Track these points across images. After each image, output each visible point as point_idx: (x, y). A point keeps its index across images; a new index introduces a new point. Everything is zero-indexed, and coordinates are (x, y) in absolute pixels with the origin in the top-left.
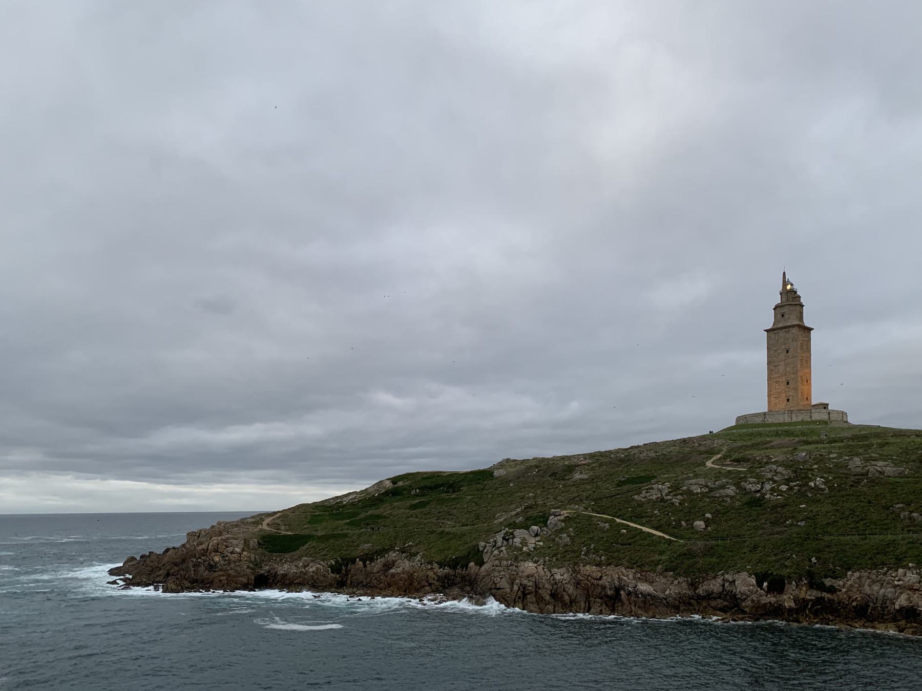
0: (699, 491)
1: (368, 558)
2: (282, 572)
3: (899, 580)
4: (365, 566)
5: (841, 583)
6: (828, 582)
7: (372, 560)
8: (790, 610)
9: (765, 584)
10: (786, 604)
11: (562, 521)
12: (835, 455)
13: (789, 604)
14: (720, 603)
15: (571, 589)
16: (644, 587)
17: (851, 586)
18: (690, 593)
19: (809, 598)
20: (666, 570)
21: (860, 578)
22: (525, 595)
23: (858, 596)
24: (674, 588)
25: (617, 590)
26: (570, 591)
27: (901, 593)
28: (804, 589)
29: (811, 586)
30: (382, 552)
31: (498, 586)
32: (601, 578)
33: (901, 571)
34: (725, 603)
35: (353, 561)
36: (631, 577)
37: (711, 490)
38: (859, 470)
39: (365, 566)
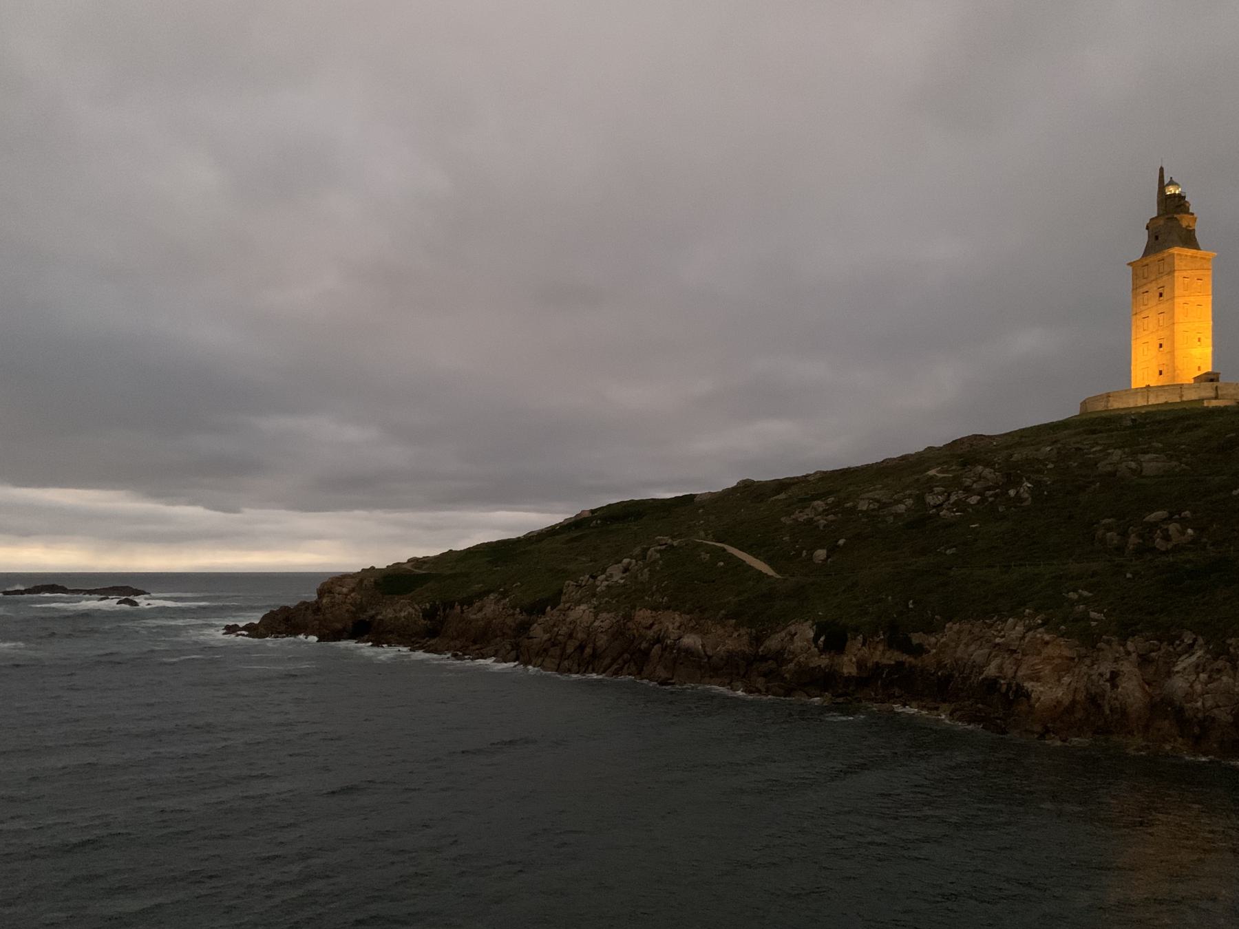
0: (865, 508)
1: (470, 603)
2: (380, 617)
3: (1003, 636)
4: (462, 612)
5: (933, 640)
6: (916, 638)
7: (470, 604)
8: (849, 679)
9: (822, 639)
10: (845, 671)
11: (659, 551)
12: (1098, 448)
13: (848, 666)
14: (771, 664)
15: (602, 641)
16: (690, 640)
17: (946, 645)
18: (746, 649)
19: (885, 661)
20: (727, 617)
21: (959, 632)
22: (554, 645)
23: (948, 661)
24: (728, 640)
25: (658, 640)
26: (598, 644)
27: (996, 656)
28: (881, 648)
29: (892, 644)
30: (482, 595)
31: (531, 634)
32: (652, 625)
33: (1011, 620)
34: (774, 666)
35: (452, 607)
36: (677, 624)
37: (883, 505)
38: (1109, 468)
39: (462, 612)
